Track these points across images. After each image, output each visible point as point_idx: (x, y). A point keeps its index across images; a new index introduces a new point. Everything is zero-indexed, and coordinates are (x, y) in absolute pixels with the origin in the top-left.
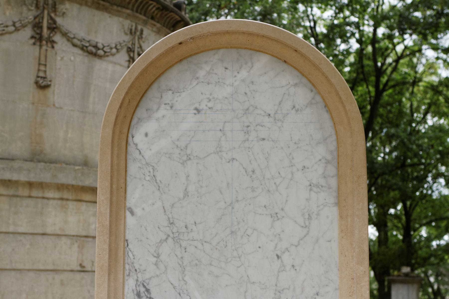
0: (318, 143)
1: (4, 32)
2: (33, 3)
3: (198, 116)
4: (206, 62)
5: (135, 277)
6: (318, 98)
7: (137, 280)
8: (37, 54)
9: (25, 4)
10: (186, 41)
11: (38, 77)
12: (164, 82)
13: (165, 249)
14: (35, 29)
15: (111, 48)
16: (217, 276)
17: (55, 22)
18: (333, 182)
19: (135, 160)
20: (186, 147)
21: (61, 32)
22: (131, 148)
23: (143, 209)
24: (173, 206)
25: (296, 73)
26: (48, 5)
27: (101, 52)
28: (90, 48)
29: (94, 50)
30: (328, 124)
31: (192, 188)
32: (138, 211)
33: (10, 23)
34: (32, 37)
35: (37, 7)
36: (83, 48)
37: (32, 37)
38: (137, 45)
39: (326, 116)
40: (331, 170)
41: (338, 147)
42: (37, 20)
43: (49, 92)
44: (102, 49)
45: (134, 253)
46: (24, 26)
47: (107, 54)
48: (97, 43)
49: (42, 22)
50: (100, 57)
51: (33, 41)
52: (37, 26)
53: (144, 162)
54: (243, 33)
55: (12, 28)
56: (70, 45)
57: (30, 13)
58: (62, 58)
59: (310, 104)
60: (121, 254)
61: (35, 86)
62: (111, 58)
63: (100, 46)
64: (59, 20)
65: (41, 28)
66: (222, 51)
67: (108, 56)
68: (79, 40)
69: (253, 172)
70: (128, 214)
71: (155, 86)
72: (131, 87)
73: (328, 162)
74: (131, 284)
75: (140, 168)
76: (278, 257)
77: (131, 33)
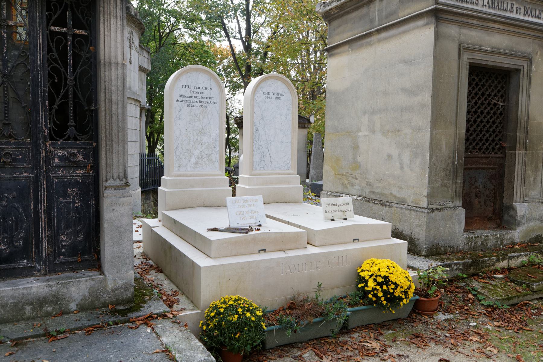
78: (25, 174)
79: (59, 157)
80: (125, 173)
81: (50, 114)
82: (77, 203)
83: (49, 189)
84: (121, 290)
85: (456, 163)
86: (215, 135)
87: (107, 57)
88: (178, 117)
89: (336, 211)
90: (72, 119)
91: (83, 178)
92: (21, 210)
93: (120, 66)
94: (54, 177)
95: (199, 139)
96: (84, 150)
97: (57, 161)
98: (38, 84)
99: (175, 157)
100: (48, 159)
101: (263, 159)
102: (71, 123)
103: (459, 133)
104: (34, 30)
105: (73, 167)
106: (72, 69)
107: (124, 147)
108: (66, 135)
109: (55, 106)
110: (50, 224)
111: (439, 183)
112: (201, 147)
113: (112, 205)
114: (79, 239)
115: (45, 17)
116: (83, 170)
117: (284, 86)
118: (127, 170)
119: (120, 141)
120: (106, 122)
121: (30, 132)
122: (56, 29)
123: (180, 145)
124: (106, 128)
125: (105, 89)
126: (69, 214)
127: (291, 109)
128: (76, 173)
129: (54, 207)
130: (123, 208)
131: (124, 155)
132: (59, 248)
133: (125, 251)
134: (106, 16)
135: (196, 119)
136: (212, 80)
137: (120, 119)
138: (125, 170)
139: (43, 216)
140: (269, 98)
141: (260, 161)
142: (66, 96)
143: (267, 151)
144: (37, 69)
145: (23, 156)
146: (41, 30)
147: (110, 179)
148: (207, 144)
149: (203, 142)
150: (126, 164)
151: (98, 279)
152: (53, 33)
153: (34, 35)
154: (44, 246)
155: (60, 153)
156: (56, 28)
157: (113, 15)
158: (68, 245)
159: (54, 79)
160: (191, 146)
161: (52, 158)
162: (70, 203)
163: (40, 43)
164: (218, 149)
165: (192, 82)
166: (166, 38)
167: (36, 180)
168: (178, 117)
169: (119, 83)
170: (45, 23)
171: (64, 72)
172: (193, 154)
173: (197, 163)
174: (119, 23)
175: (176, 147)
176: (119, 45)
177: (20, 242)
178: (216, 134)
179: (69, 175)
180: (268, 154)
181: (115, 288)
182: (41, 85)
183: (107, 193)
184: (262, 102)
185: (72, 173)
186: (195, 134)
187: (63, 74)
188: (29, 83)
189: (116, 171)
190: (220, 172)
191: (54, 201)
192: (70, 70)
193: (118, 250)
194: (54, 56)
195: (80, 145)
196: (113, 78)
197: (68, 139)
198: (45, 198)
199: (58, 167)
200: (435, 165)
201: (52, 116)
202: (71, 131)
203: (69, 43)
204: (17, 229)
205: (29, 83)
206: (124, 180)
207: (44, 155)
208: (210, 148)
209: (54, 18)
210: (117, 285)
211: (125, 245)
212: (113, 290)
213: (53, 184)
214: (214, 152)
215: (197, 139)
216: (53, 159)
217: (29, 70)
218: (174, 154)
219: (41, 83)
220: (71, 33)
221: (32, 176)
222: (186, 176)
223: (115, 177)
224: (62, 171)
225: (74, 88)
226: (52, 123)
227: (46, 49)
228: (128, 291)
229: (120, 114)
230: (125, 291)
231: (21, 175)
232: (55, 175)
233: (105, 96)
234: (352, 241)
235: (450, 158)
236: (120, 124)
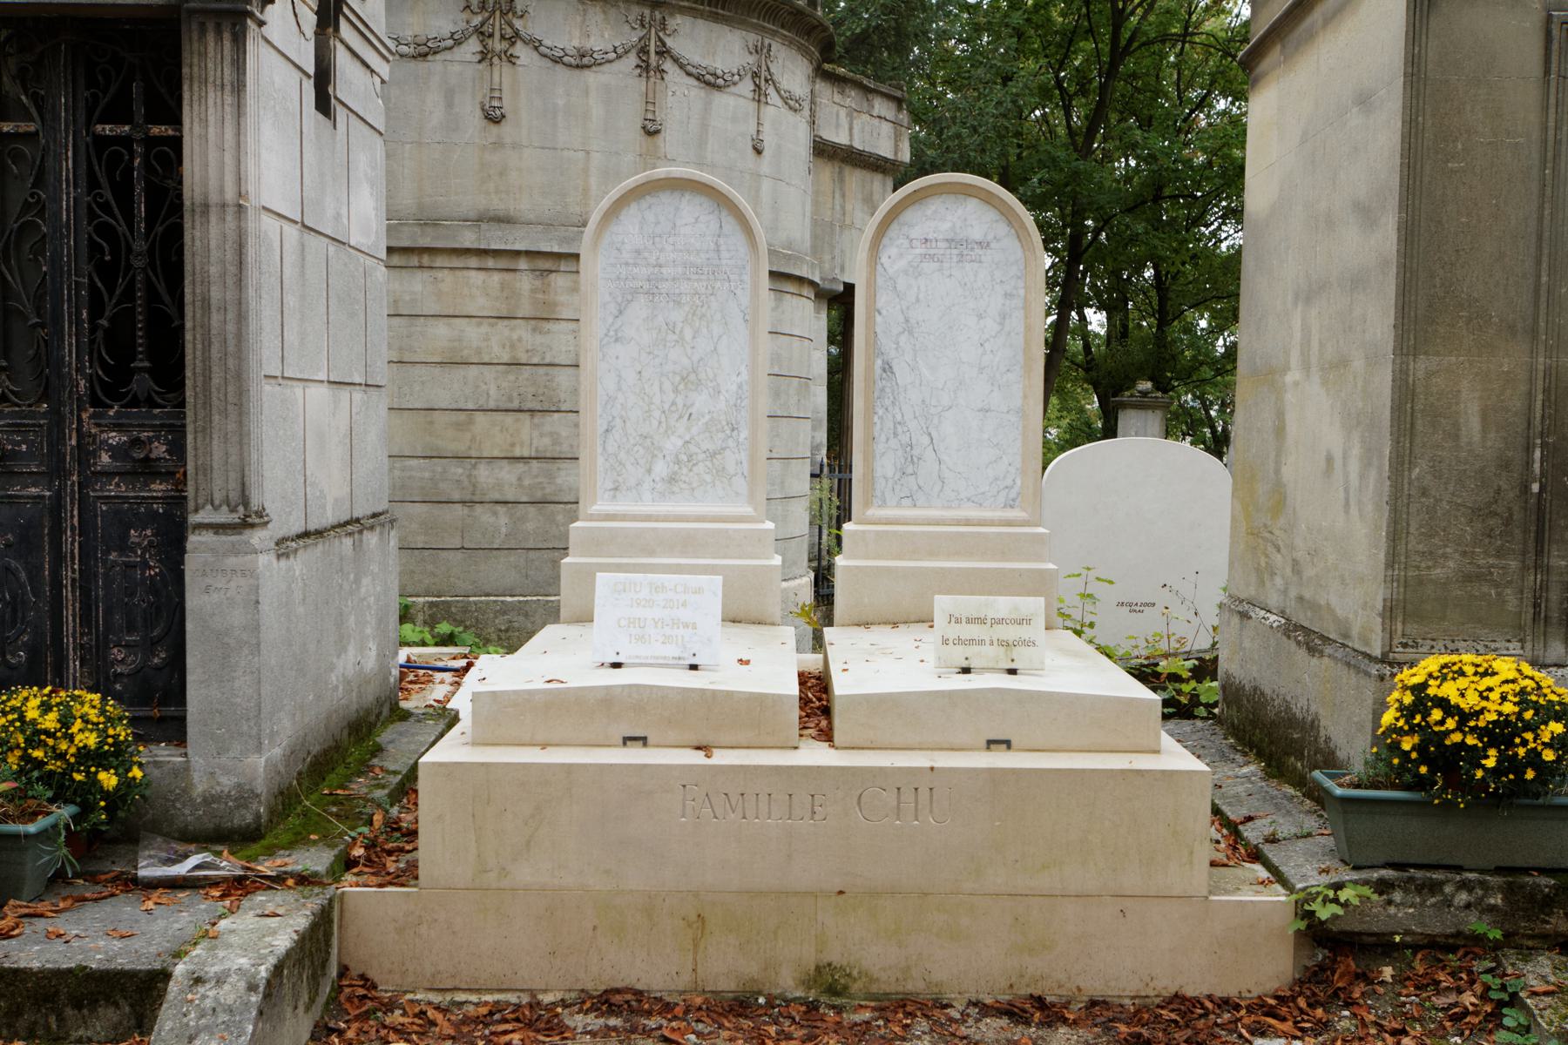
6: (1013, 231)
8: (644, 89)
13: (903, 339)
17: (664, 44)
22: (879, 267)
24: (908, 308)
27: (720, 81)
28: (708, 77)
31: (921, 296)
33: (610, 48)
34: (638, 66)
35: (643, 26)
36: (698, 78)
37: (638, 66)
38: (764, 68)
43: (659, 139)
50: (719, 88)
51: (639, 71)
52: (643, 51)
55: (614, 55)
57: (633, 33)
62: (733, 89)
63: (719, 72)
64: (669, 42)
65: (648, 53)
78: (33, 490)
79: (111, 448)
80: (243, 491)
81: (92, 342)
82: (150, 568)
83: (85, 528)
84: (226, 804)
85: (1535, 487)
86: (734, 388)
87: (197, 190)
88: (612, 333)
89: (981, 642)
90: (141, 353)
91: (168, 504)
92: (23, 575)
93: (231, 211)
94: (99, 498)
95: (680, 400)
96: (169, 432)
97: (105, 458)
98: (61, 268)
99: (600, 460)
100: (85, 453)
101: (910, 470)
102: (142, 363)
103: (1547, 372)
104: (55, 141)
105: (142, 474)
106: (143, 225)
107: (240, 423)
108: (128, 392)
109: (104, 322)
110: (86, 617)
111: (1451, 564)
112: (688, 429)
113: (204, 574)
114: (156, 660)
115: (81, 104)
116: (167, 482)
117: (991, 215)
118: (247, 483)
119: (230, 408)
120: (195, 358)
121: (46, 388)
122: (107, 129)
123: (618, 422)
124: (194, 374)
125: (194, 274)
126: (132, 595)
127: (1022, 292)
128: (150, 491)
129: (96, 575)
130: (233, 584)
131: (241, 444)
132: (107, 678)
133: (239, 700)
134: (196, 88)
135: (672, 337)
136: (724, 213)
137: (231, 348)
138: (243, 484)
139: (70, 594)
140: (932, 257)
142: (129, 294)
143: (926, 440)
144: (61, 233)
145: (30, 444)
146: (71, 138)
147: (203, 507)
148: (707, 417)
149: (693, 410)
150: (247, 469)
151: (170, 766)
152: (101, 142)
153: (55, 151)
154: (71, 671)
155: (114, 438)
156: (108, 127)
157: (214, 81)
158: (129, 675)
159: (103, 254)
160: (655, 423)
161: (94, 450)
162: (133, 566)
163: (67, 169)
164: (744, 434)
165: (658, 223)
166: (1146, 13)
167: (58, 499)
168: (612, 333)
169: (230, 256)
170: (82, 119)
171: (124, 235)
172: (660, 449)
173: (672, 479)
174: (229, 99)
175: (605, 427)
176: (229, 159)
177: (20, 656)
178: (740, 386)
179: (132, 494)
180: (929, 453)
181: (213, 796)
182: (69, 271)
183: (193, 539)
184: (906, 272)
185: (141, 491)
186: (667, 386)
187: (122, 239)
188: (44, 269)
189: (221, 484)
190: (748, 510)
191: (96, 559)
192: (139, 228)
193: (219, 695)
194: (102, 197)
195: (161, 418)
196: (213, 244)
197: (135, 402)
198: (76, 551)
199: (108, 474)
200: (1424, 492)
201: (96, 346)
202: (142, 383)
203: (137, 162)
204: (14, 623)
205: (44, 269)
206: (241, 509)
207: (74, 442)
208: (718, 431)
209: (103, 102)
210: (218, 789)
211: (237, 684)
212: (209, 800)
213: (96, 516)
214: (731, 443)
215: (674, 403)
216: (95, 455)
217: (44, 236)
218: (599, 450)
219: (69, 266)
220: (139, 136)
221: (48, 493)
222: (657, 520)
223: (217, 502)
224: (118, 485)
225: (147, 275)
226: (96, 364)
227: (83, 182)
228: (246, 807)
229: (230, 337)
230: (237, 807)
231: (24, 493)
232: (100, 494)
233: (194, 293)
234: (984, 744)
235: (1505, 465)
236: (231, 363)
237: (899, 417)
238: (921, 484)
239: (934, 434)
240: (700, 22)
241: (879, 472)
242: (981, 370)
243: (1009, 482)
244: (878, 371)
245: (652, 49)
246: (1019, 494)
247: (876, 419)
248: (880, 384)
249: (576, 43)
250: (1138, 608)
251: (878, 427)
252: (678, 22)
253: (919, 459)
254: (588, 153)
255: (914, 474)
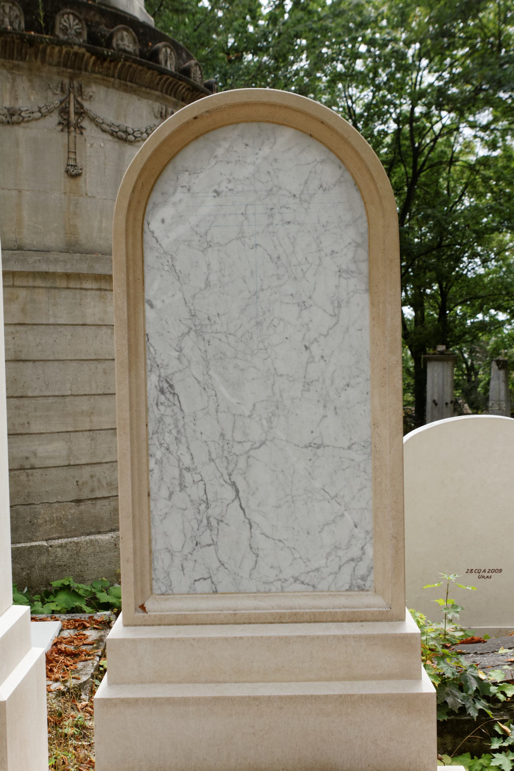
0: (347, 226)
1: (30, 119)
2: (58, 86)
3: (218, 199)
4: (225, 139)
5: (158, 373)
6: (347, 176)
7: (160, 376)
8: (66, 141)
9: (50, 88)
10: (202, 115)
11: (68, 165)
12: (179, 162)
13: (188, 343)
14: (62, 114)
15: (142, 133)
16: (243, 370)
17: (82, 107)
18: (364, 267)
19: (151, 248)
20: (206, 233)
21: (89, 117)
22: (148, 237)
23: (163, 301)
24: (194, 297)
25: (323, 148)
26: (73, 88)
27: (131, 138)
28: (120, 133)
29: (124, 135)
30: (358, 204)
31: (213, 278)
32: (158, 304)
33: (36, 109)
34: (60, 123)
35: (62, 90)
36: (112, 134)
37: (60, 123)
39: (356, 195)
40: (362, 254)
41: (369, 229)
42: (63, 105)
44: (133, 134)
45: (155, 348)
46: (50, 112)
47: (137, 139)
48: (127, 127)
49: (69, 107)
50: (131, 142)
51: (61, 127)
52: (64, 111)
53: (162, 251)
54: (264, 104)
55: (39, 115)
56: (100, 131)
57: (55, 98)
58: (92, 145)
59: (339, 182)
60: (141, 349)
61: (66, 175)
63: (130, 130)
64: (86, 105)
65: (68, 113)
66: (241, 126)
67: (138, 141)
68: (108, 125)
69: (279, 258)
70: (147, 306)
71: (170, 167)
72: (144, 169)
73: (358, 245)
74: (153, 379)
75: (157, 257)
76: (306, 348)
77: (161, 116)
101: (206, 538)
141: (190, 546)
143: (229, 493)
237: (187, 461)
238: (224, 559)
239: (241, 485)
240: (111, 90)
241: (159, 545)
242: (308, 385)
243: (355, 552)
244: (153, 392)
245: (72, 109)
246: (371, 569)
247: (152, 464)
248: (155, 413)
249: (7, 104)
250: (486, 575)
251: (155, 476)
252: (93, 89)
253: (219, 521)
254: (20, 191)
255: (213, 544)
